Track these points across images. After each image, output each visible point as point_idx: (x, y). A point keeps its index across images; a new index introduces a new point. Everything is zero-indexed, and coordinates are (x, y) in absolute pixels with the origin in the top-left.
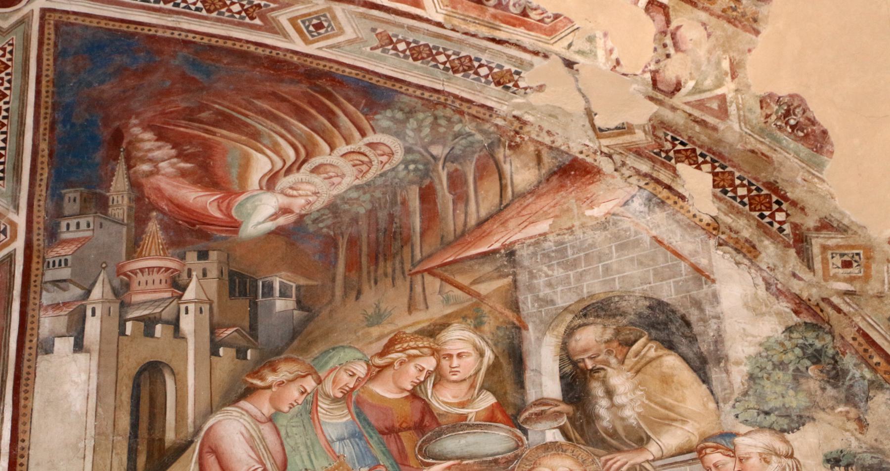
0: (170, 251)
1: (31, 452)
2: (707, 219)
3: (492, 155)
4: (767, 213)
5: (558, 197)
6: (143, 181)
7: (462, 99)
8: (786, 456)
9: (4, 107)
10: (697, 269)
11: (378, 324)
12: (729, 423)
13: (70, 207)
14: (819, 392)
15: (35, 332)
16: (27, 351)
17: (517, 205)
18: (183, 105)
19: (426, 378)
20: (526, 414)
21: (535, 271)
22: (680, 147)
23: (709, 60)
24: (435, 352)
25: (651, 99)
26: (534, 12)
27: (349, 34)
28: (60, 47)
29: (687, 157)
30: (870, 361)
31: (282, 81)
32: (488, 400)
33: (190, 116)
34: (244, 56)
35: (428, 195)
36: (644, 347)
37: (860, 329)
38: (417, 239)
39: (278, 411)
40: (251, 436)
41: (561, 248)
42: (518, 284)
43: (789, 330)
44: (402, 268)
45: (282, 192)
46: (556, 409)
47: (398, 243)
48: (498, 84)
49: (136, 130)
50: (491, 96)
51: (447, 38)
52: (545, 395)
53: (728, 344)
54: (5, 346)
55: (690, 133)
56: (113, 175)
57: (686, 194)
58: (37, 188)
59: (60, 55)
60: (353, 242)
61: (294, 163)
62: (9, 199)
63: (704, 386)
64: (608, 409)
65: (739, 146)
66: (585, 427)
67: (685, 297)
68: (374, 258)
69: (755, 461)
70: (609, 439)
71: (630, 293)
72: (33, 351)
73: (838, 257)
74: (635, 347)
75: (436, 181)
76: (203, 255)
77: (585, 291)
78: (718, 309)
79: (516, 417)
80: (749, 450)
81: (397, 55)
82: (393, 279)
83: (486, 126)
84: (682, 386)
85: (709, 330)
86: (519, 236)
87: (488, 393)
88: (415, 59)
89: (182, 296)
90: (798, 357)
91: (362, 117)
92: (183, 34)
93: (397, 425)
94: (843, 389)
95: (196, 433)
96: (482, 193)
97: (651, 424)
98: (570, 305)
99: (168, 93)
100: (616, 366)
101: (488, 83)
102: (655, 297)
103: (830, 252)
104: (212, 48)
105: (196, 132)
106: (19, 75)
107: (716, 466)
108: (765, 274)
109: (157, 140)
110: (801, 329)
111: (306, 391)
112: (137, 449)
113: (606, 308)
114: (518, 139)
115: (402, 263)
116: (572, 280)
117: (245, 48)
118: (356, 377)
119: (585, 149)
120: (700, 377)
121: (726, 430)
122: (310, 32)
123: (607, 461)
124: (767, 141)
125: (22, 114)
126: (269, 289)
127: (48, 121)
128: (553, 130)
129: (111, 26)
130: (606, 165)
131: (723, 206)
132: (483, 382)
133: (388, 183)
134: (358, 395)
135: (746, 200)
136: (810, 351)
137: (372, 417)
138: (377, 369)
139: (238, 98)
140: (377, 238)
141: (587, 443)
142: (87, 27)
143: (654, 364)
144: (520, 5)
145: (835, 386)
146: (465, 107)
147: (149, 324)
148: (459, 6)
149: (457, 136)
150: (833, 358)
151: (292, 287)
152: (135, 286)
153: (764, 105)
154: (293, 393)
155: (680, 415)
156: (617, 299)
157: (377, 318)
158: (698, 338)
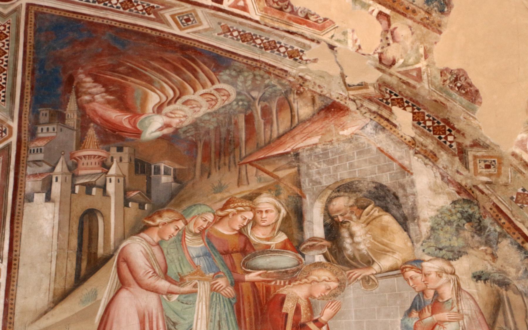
0: (101, 146)
1: (21, 258)
2: (409, 139)
3: (287, 98)
4: (443, 136)
5: (324, 124)
6: (86, 105)
7: (270, 65)
9: (5, 59)
10: (403, 167)
11: (220, 192)
12: (419, 254)
13: (43, 119)
14: (470, 238)
15: (23, 189)
16: (18, 200)
17: (301, 127)
18: (109, 62)
20: (304, 246)
21: (310, 165)
22: (394, 97)
23: (412, 48)
24: (252, 209)
25: (378, 69)
26: (312, 17)
27: (205, 25)
28: (37, 26)
29: (398, 103)
30: (499, 222)
31: (166, 51)
32: (282, 237)
33: (113, 69)
34: (144, 36)
35: (249, 120)
36: (372, 210)
37: (494, 204)
38: (243, 145)
39: (163, 239)
40: (147, 253)
41: (325, 153)
42: (301, 172)
44: (235, 161)
45: (166, 115)
46: (321, 243)
48: (291, 57)
49: (82, 76)
50: (286, 64)
51: (262, 30)
52: (315, 235)
53: (419, 210)
54: (5, 197)
55: (400, 89)
56: (68, 101)
57: (397, 124)
58: (24, 107)
59: (37, 31)
60: (206, 145)
61: (173, 99)
62: (8, 113)
63: (405, 233)
64: (351, 244)
65: (428, 98)
66: (337, 253)
67: (396, 182)
68: (219, 154)
69: (433, 276)
70: (351, 261)
71: (365, 179)
72: (22, 200)
73: (483, 162)
74: (367, 210)
75: (255, 112)
76: (120, 149)
77: (339, 177)
78: (414, 190)
81: (233, 39)
82: (229, 167)
83: (284, 81)
84: (393, 233)
85: (409, 202)
86: (301, 145)
87: (283, 233)
88: (243, 41)
90: (459, 218)
91: (212, 73)
92: (109, 21)
93: (230, 250)
94: (484, 237)
96: (280, 119)
97: (375, 253)
98: (330, 185)
99: (100, 55)
100: (355, 220)
101: (285, 56)
102: (378, 182)
103: (478, 160)
104: (126, 30)
105: (116, 79)
106: (14, 42)
107: (411, 278)
108: (441, 171)
109: (94, 82)
110: (461, 202)
111: (178, 228)
113: (351, 187)
114: (302, 90)
115: (234, 157)
116: (331, 171)
117: (145, 31)
118: (207, 222)
119: (340, 96)
120: (403, 227)
122: (183, 23)
123: (350, 273)
124: (444, 95)
126: (158, 170)
127: (30, 68)
128: (322, 84)
129: (67, 15)
130: (352, 106)
131: (418, 131)
132: (280, 227)
133: (227, 112)
134: (208, 232)
135: (431, 128)
136: (465, 215)
137: (216, 244)
138: (220, 218)
139: (140, 60)
140: (220, 143)
141: (339, 263)
142: (53, 15)
143: (378, 220)
144: (304, 12)
145: (479, 235)
146: (271, 70)
147: (88, 187)
148: (269, 12)
149: (267, 86)
150: (479, 219)
151: (171, 169)
152: (80, 165)
153: (443, 74)
155: (392, 249)
156: (357, 182)
157: (220, 189)
158: (403, 206)
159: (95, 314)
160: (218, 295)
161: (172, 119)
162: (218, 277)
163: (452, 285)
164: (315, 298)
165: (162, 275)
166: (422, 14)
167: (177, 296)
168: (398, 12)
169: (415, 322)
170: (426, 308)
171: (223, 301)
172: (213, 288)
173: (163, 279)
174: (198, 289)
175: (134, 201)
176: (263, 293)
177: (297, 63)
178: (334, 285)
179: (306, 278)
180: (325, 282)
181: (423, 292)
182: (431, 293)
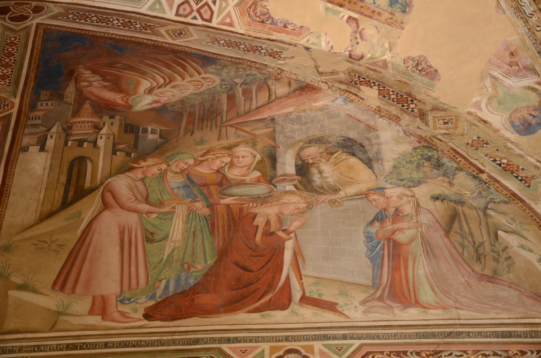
0: (95, 115)
1: (12, 189)
2: (374, 107)
5: (299, 98)
6: (84, 89)
7: (252, 62)
8: (411, 196)
11: (201, 144)
12: (382, 184)
13: (42, 97)
14: (429, 172)
17: (277, 101)
18: (108, 61)
19: (225, 166)
20: (277, 179)
23: (378, 44)
25: (349, 61)
26: (290, 25)
27: (196, 37)
30: (456, 160)
32: (257, 174)
33: (111, 65)
34: (141, 44)
35: (231, 98)
36: (340, 155)
37: (451, 148)
38: (224, 114)
39: (146, 177)
40: (131, 186)
41: (299, 119)
42: (275, 131)
43: (415, 148)
45: (156, 95)
46: (292, 178)
47: (215, 115)
48: (271, 56)
50: (267, 60)
52: (287, 172)
57: (365, 98)
58: (27, 91)
59: (45, 41)
60: (191, 115)
63: (370, 170)
66: (307, 185)
67: (363, 136)
69: (394, 198)
70: (319, 190)
72: (18, 151)
74: (335, 155)
75: (236, 92)
77: (310, 134)
78: (379, 141)
79: (271, 181)
80: (392, 194)
81: (220, 45)
82: (211, 128)
83: (264, 72)
86: (278, 113)
89: (99, 132)
95: (102, 183)
96: (259, 97)
101: (265, 55)
104: (124, 40)
105: (113, 72)
107: (374, 200)
108: (403, 128)
111: (161, 169)
112: (69, 190)
114: (279, 77)
115: (216, 122)
117: (141, 41)
120: (368, 166)
121: (380, 187)
122: (176, 36)
123: (317, 198)
124: (407, 77)
125: (22, 63)
126: (145, 131)
127: (36, 65)
129: (72, 31)
130: (324, 86)
133: (211, 92)
135: (395, 100)
136: (425, 156)
140: (204, 113)
141: (307, 191)
142: (60, 31)
143: (345, 161)
144: (283, 22)
145: (437, 170)
146: (253, 64)
147: (80, 143)
148: (252, 25)
149: (247, 75)
150: (437, 159)
152: (74, 127)
153: (406, 62)
154: (155, 170)
156: (326, 137)
157: (202, 142)
158: (368, 151)
159: (78, 227)
160: (194, 214)
161: (161, 98)
162: (196, 201)
163: (412, 204)
164: (284, 214)
165: (143, 201)
166: (387, 15)
167: (156, 215)
168: (366, 15)
169: (376, 229)
170: (387, 220)
171: (199, 218)
172: (190, 209)
173: (144, 203)
174: (176, 210)
175: (120, 150)
176: (236, 212)
177: (276, 59)
178: (303, 205)
179: (277, 201)
180: (294, 204)
181: (385, 210)
182: (392, 210)
